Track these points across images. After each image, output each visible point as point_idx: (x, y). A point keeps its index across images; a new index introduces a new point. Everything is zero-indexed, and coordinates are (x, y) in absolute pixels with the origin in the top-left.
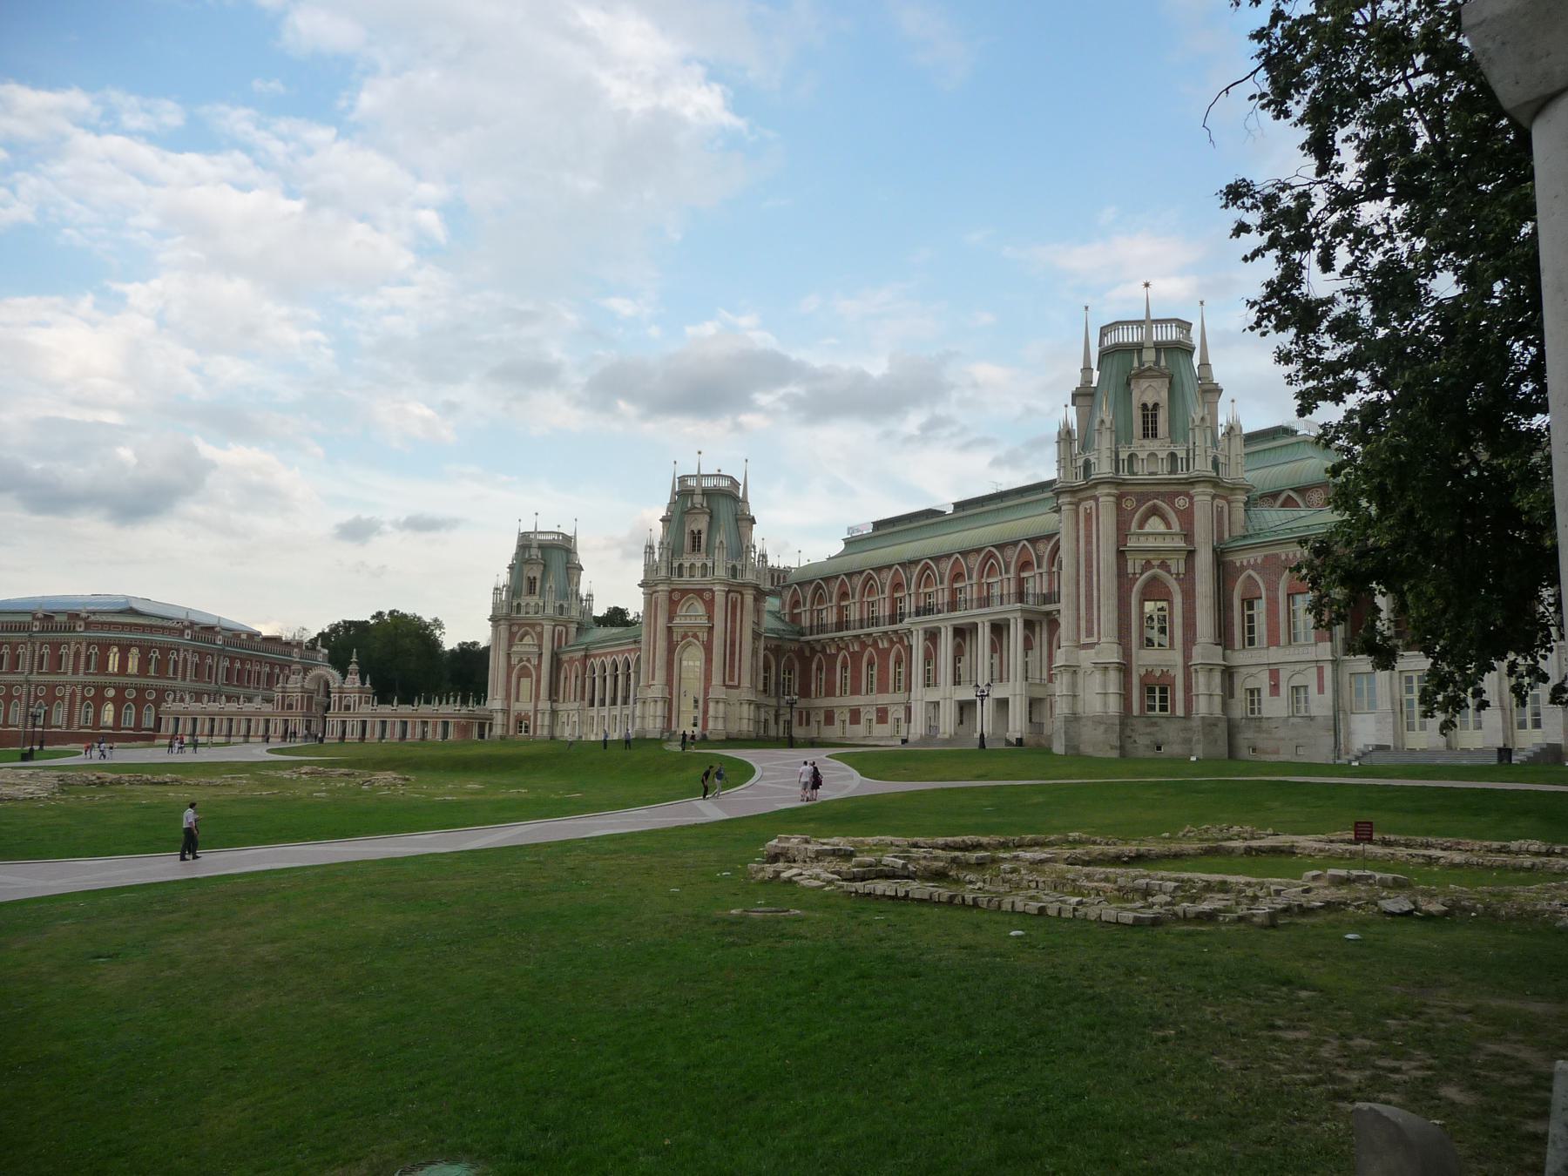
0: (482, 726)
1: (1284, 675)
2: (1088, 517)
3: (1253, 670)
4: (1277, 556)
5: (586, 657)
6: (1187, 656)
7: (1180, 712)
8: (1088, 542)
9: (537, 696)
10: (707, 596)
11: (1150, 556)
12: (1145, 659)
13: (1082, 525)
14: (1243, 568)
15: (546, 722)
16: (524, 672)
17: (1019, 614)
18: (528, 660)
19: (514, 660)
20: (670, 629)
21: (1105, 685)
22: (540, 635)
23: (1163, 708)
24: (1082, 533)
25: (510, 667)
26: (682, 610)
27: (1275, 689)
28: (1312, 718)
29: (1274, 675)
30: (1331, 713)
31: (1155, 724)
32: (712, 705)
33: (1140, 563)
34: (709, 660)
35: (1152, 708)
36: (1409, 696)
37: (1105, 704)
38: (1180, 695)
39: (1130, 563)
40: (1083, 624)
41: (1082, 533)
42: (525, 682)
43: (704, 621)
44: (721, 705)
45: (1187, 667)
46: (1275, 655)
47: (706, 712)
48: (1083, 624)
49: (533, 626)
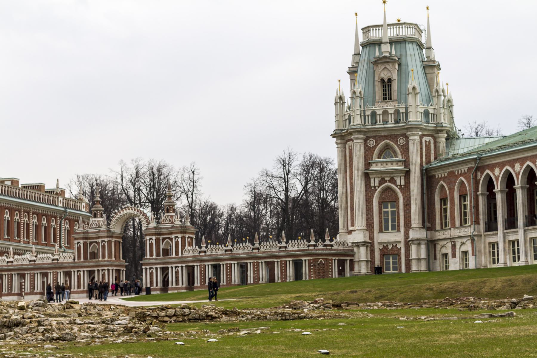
0: (341, 263)
15: (423, 255)
18: (392, 180)
19: (374, 182)
22: (406, 150)
25: (369, 190)
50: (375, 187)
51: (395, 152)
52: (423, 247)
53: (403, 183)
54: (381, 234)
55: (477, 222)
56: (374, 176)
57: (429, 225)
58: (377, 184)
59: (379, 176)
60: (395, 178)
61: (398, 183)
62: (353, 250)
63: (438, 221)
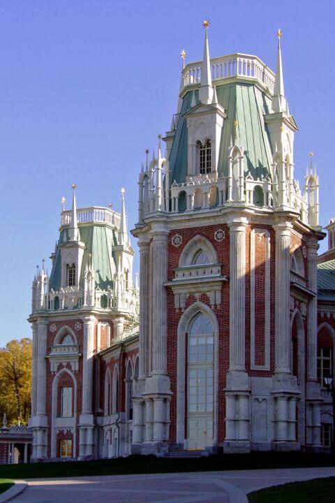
5: (124, 355)
9: (79, 410)
10: (218, 236)
15: (89, 442)
16: (65, 382)
18: (69, 366)
19: (54, 368)
20: (168, 290)
22: (81, 336)
25: (49, 376)
26: (185, 262)
32: (229, 402)
34: (224, 334)
42: (68, 393)
43: (216, 274)
44: (243, 402)
47: (221, 413)
49: (71, 323)
50: (54, 372)
51: (73, 338)
52: (90, 432)
53: (77, 368)
54: (59, 419)
55: (123, 410)
56: (54, 361)
57: (100, 410)
58: (56, 370)
59: (58, 361)
60: (71, 364)
61: (73, 369)
62: (31, 435)
63: (106, 407)
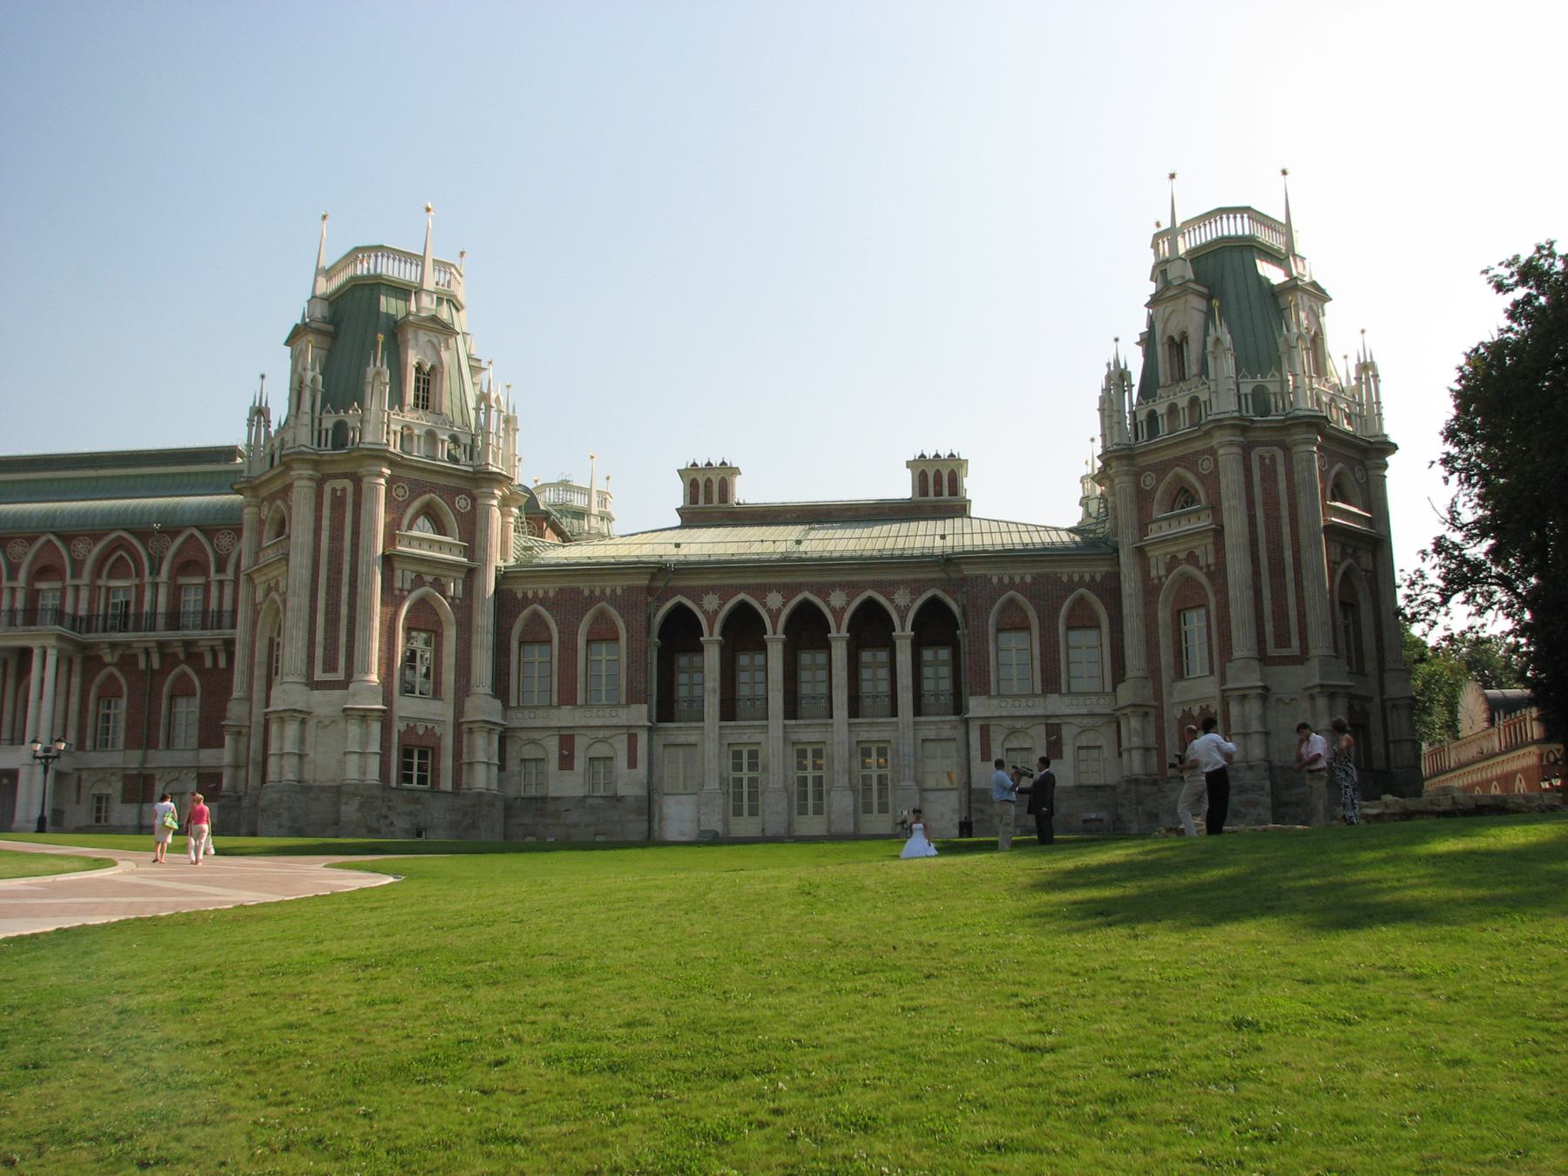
1: (580, 743)
2: (338, 503)
3: (536, 735)
4: (579, 592)
6: (459, 711)
7: (446, 784)
8: (336, 536)
11: (423, 569)
12: (408, 708)
13: (326, 512)
14: (526, 602)
17: (53, 642)
21: (365, 741)
23: (422, 780)
24: (326, 522)
27: (566, 762)
28: (617, 799)
29: (567, 742)
30: (643, 793)
31: (417, 801)
33: (410, 576)
35: (408, 779)
36: (738, 775)
37: (363, 771)
38: (447, 763)
39: (398, 573)
40: (319, 652)
41: (326, 522)
45: (458, 725)
46: (565, 717)
48: (319, 652)
